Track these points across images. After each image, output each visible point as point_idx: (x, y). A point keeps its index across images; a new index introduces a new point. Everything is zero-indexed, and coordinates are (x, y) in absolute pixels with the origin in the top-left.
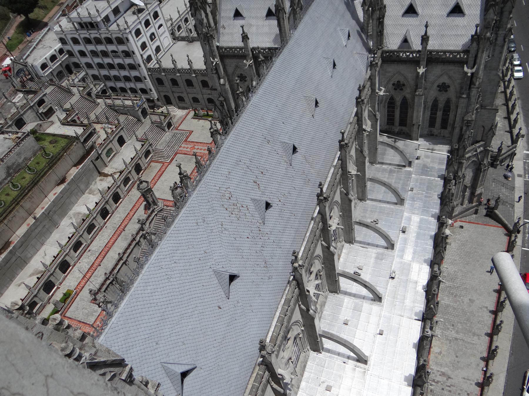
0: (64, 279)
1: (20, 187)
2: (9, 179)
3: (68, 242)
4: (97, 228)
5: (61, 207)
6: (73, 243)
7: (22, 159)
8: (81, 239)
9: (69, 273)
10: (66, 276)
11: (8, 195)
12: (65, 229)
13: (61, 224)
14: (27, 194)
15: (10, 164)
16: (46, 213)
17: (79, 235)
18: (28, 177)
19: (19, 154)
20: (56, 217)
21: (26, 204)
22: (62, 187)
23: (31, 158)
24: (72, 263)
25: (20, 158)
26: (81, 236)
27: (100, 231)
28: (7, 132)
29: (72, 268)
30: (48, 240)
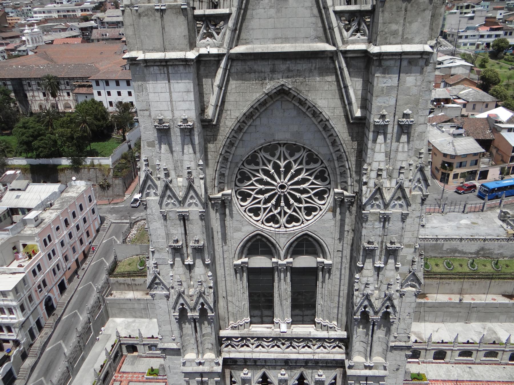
0: (429, 363)
1: (475, 269)
2: (473, 256)
3: (464, 343)
4: (496, 359)
5: (486, 313)
6: (466, 348)
7: (499, 252)
8: (474, 353)
9: (437, 363)
10: (433, 363)
11: (461, 265)
12: (472, 332)
13: (472, 324)
14: (475, 279)
15: (486, 247)
16: (472, 306)
17: (477, 348)
18: (489, 268)
19: (501, 247)
20: (474, 315)
21: (467, 284)
22: (506, 301)
23: (506, 257)
24: (447, 359)
25: (499, 250)
26: (478, 350)
27: (495, 364)
28: (508, 224)
29: (443, 363)
30: (449, 324)
